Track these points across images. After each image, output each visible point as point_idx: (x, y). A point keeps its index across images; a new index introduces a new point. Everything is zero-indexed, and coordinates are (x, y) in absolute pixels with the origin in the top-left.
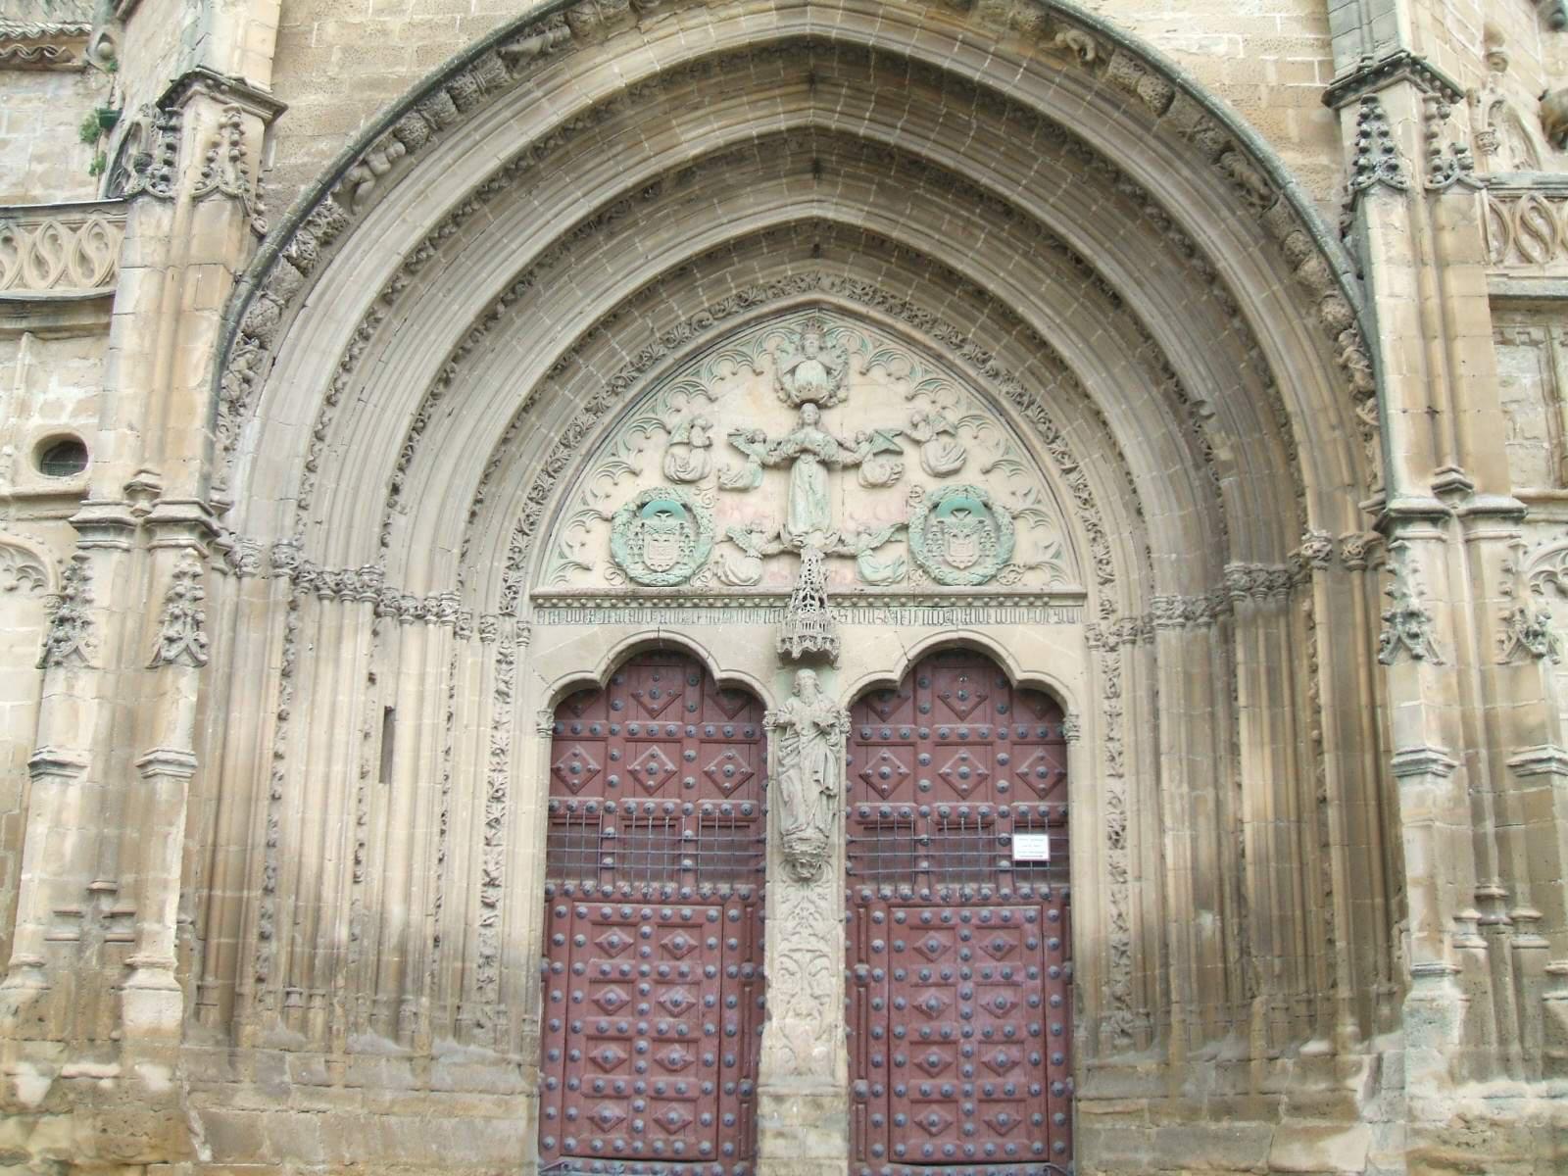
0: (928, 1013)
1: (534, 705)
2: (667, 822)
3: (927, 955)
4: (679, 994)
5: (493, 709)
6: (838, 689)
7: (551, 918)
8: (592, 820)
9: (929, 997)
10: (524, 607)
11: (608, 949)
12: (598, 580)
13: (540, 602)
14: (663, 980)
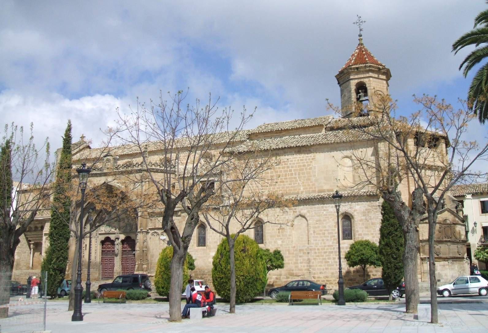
0: (128, 266)
1: (99, 242)
2: (109, 251)
3: (127, 261)
4: (110, 265)
5: (96, 243)
6: (120, 240)
7: (102, 259)
8: (105, 251)
9: (128, 265)
10: (98, 235)
11: (106, 262)
12: (103, 232)
13: (100, 234)
14: (110, 264)
